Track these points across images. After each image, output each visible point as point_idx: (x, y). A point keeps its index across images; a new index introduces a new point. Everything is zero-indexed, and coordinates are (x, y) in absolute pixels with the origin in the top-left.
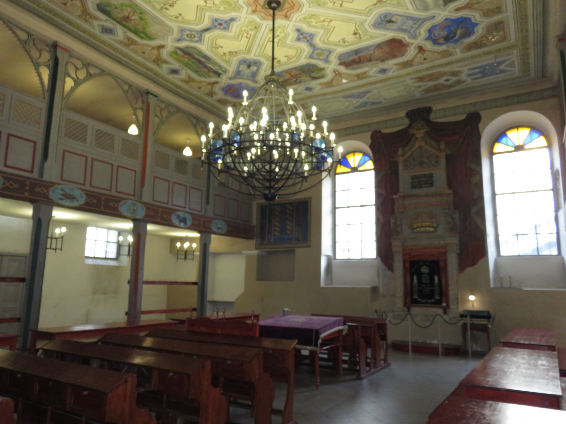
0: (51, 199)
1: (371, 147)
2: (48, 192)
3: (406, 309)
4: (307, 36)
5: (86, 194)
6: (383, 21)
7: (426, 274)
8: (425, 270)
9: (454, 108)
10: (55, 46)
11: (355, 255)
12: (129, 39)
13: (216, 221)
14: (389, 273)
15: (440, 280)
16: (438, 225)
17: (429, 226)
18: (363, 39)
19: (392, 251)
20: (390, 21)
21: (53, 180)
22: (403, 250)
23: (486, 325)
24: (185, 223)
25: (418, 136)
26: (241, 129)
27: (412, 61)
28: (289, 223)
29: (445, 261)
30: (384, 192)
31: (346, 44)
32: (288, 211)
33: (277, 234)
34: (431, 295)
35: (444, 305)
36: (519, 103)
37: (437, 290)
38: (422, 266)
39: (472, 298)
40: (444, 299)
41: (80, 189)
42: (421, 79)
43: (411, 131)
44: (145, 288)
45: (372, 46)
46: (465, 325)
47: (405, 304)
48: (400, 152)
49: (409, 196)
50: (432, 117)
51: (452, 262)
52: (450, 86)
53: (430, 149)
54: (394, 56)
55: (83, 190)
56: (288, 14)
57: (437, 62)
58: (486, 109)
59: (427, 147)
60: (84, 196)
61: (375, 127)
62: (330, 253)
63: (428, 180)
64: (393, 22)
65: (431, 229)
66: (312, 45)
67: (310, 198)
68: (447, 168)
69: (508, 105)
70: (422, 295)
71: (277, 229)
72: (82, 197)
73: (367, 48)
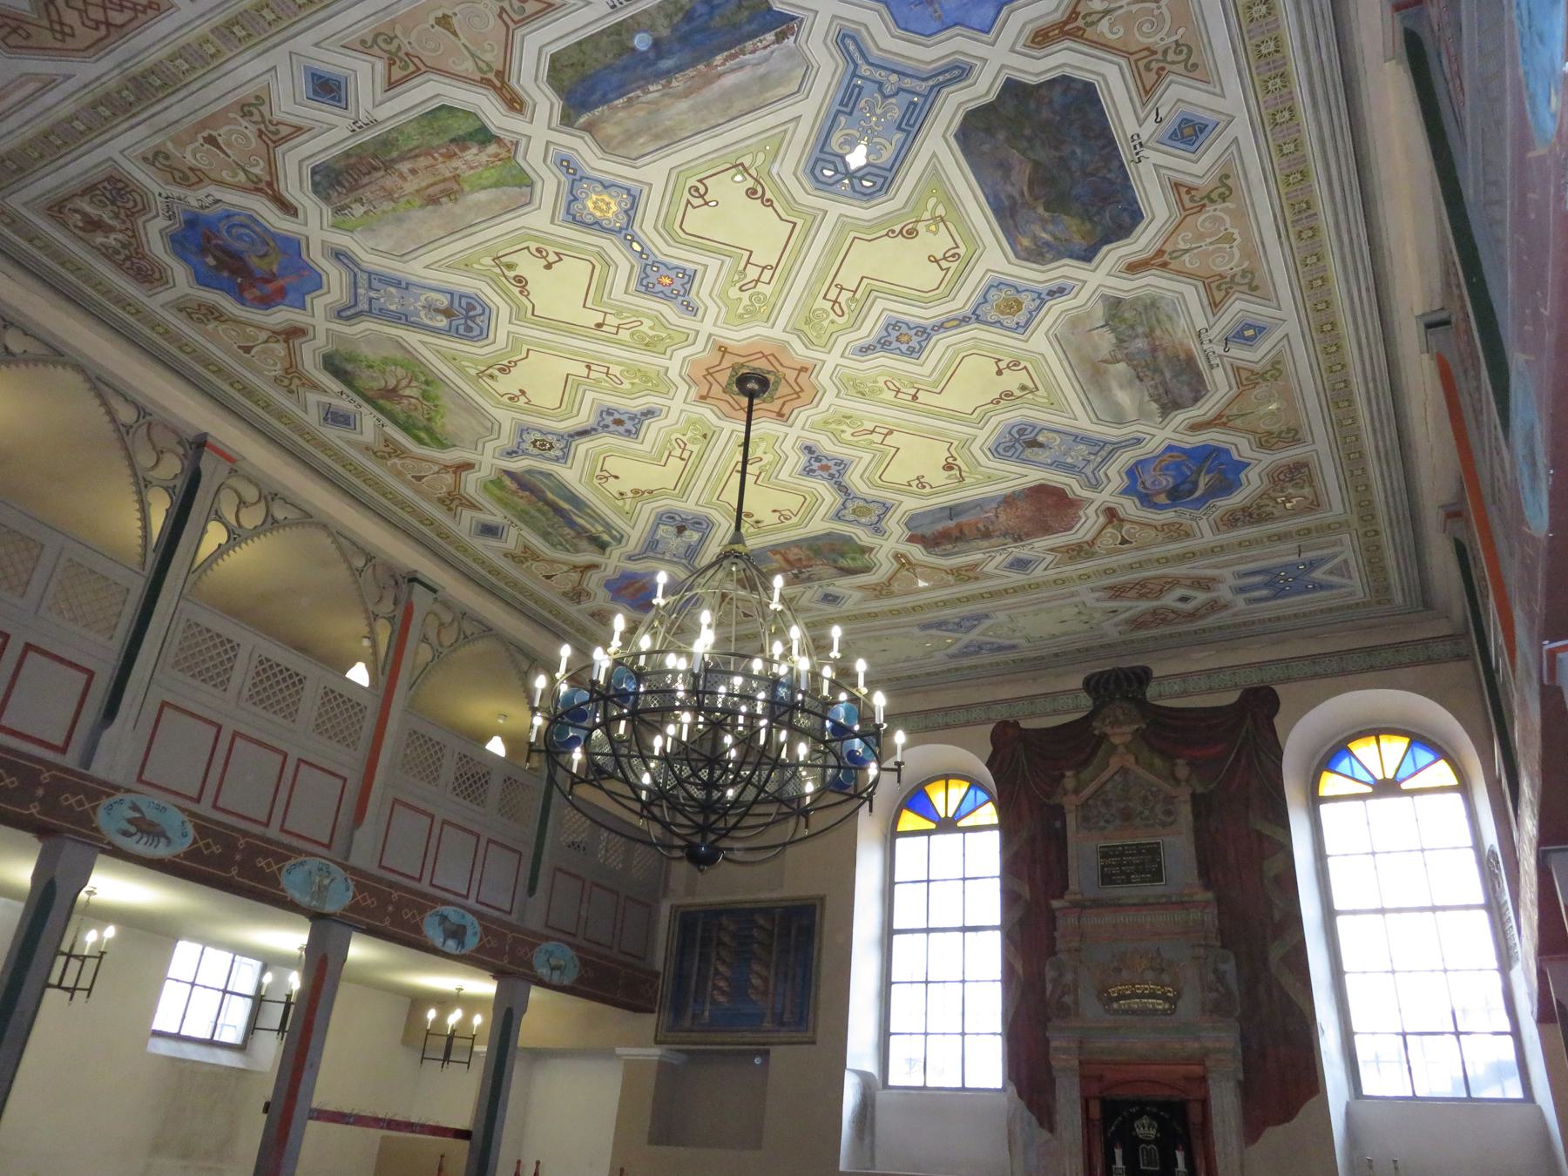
0: (97, 830)
1: (989, 765)
2: (94, 809)
4: (831, 464)
5: (197, 827)
6: (1017, 440)
7: (1148, 1143)
8: (1145, 1129)
9: (1208, 673)
10: (200, 444)
11: (944, 1076)
12: (388, 441)
13: (551, 945)
14: (1045, 1135)
15: (1190, 1161)
16: (1179, 995)
17: (1153, 995)
18: (968, 480)
19: (1049, 1068)
20: (1034, 444)
21: (117, 777)
22: (1081, 1063)
24: (461, 943)
25: (1116, 740)
26: (642, 661)
27: (1092, 543)
28: (756, 968)
29: (1205, 1102)
30: (1026, 891)
31: (928, 490)
32: (755, 932)
33: (721, 999)
36: (1372, 668)
38: (1139, 1116)
41: (183, 810)
42: (1117, 592)
43: (1098, 727)
44: (313, 1127)
45: (992, 499)
48: (1069, 782)
49: (1098, 904)
50: (1151, 692)
51: (1225, 1104)
52: (1193, 616)
53: (1151, 778)
54: (1047, 530)
55: (192, 814)
56: (786, 410)
57: (1157, 551)
58: (1288, 680)
59: (1140, 771)
60: (191, 832)
61: (1002, 713)
62: (871, 1066)
63: (1148, 863)
64: (1041, 445)
65: (1161, 1005)
66: (842, 489)
67: (822, 899)
68: (1199, 833)
69: (1344, 672)
71: (722, 984)
72: (185, 835)
73: (979, 504)
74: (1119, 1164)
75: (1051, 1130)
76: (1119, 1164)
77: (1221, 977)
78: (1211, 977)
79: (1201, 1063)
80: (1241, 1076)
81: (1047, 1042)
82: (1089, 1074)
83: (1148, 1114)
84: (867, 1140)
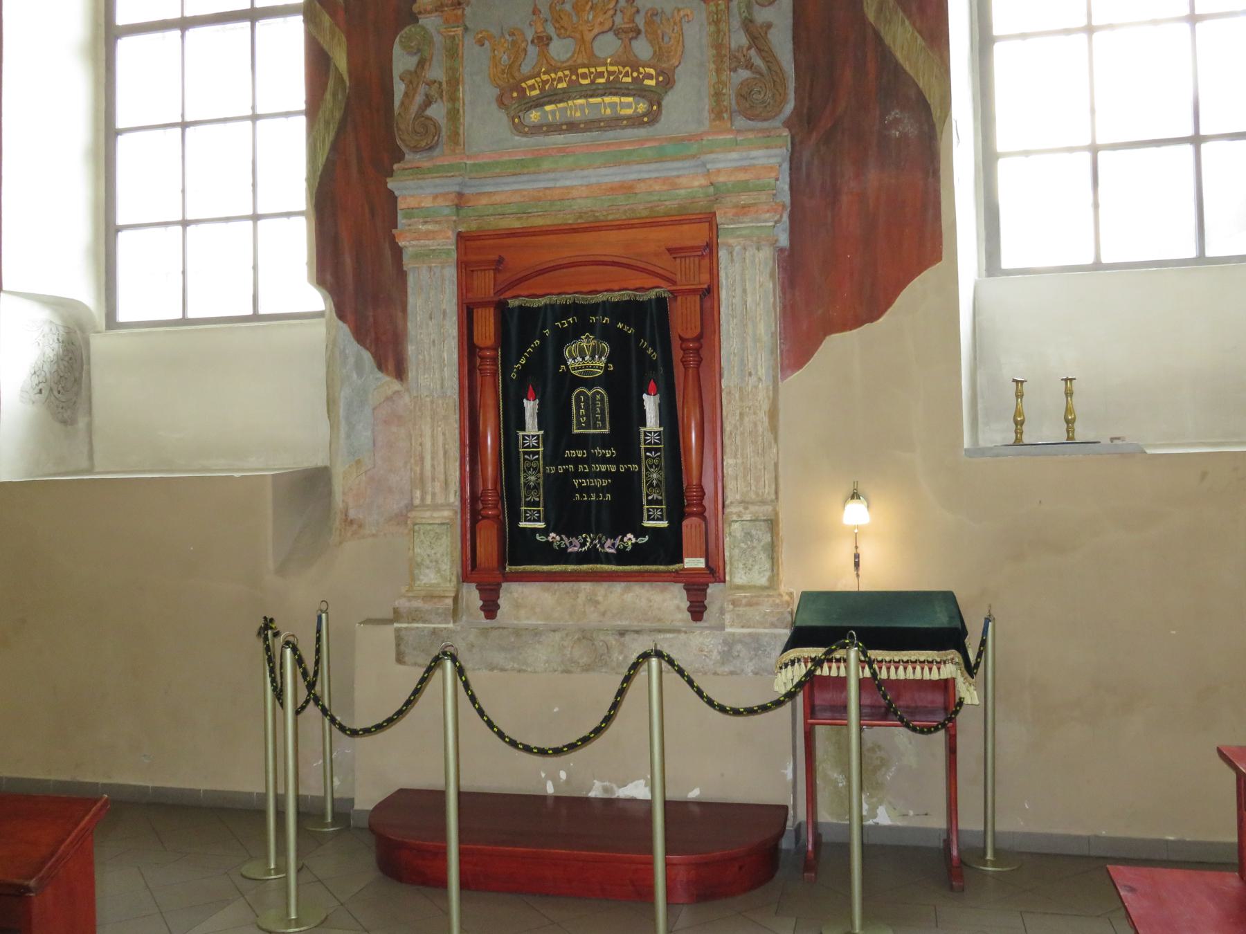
3: (472, 596)
8: (586, 357)
11: (219, 297)
15: (669, 414)
16: (668, 82)
17: (614, 88)
19: (398, 252)
22: (461, 237)
23: (946, 686)
29: (709, 293)
34: (624, 514)
35: (694, 563)
37: (652, 475)
38: (574, 334)
39: (856, 514)
40: (690, 527)
46: (817, 696)
47: (471, 569)
65: (630, 106)
70: (568, 512)
74: (532, 426)
75: (400, 372)
76: (532, 426)
77: (757, 36)
78: (739, 39)
79: (709, 219)
80: (784, 240)
81: (392, 199)
82: (477, 253)
83: (591, 329)
84: (82, 423)
